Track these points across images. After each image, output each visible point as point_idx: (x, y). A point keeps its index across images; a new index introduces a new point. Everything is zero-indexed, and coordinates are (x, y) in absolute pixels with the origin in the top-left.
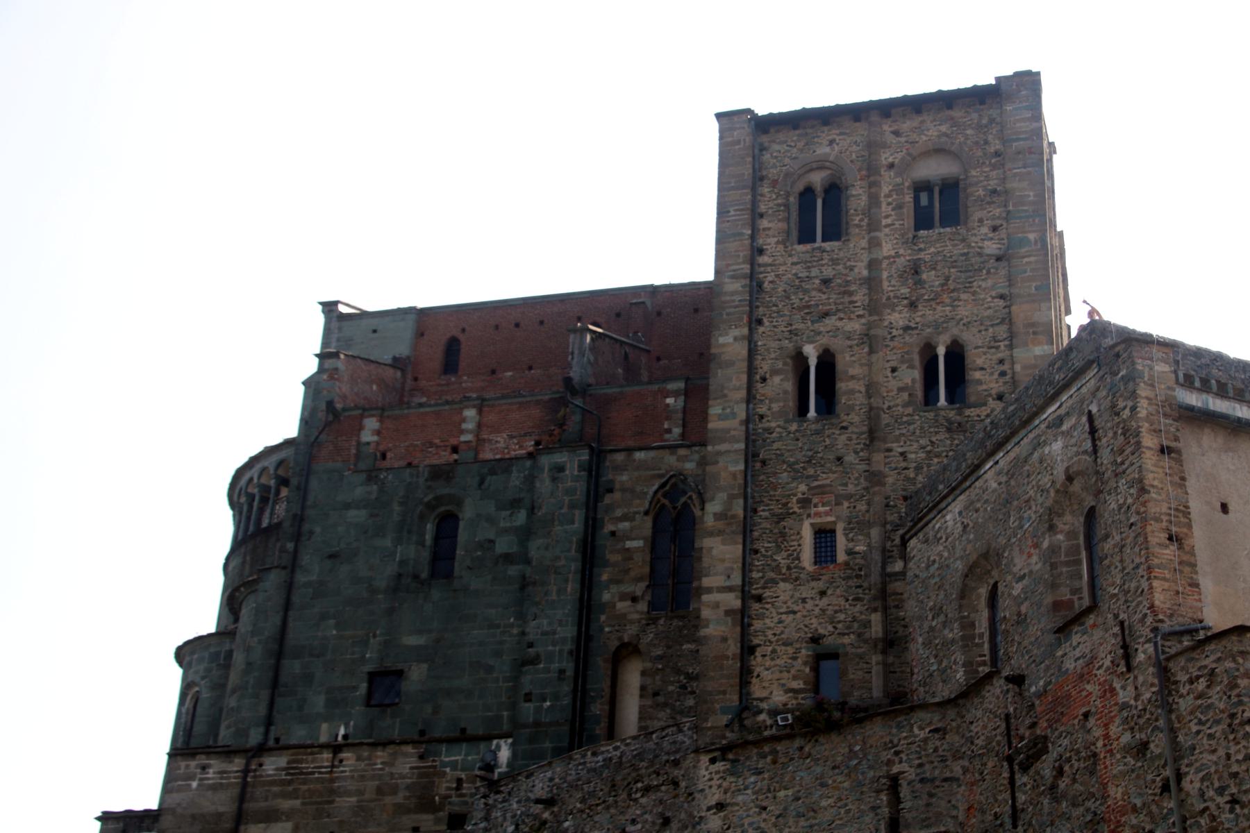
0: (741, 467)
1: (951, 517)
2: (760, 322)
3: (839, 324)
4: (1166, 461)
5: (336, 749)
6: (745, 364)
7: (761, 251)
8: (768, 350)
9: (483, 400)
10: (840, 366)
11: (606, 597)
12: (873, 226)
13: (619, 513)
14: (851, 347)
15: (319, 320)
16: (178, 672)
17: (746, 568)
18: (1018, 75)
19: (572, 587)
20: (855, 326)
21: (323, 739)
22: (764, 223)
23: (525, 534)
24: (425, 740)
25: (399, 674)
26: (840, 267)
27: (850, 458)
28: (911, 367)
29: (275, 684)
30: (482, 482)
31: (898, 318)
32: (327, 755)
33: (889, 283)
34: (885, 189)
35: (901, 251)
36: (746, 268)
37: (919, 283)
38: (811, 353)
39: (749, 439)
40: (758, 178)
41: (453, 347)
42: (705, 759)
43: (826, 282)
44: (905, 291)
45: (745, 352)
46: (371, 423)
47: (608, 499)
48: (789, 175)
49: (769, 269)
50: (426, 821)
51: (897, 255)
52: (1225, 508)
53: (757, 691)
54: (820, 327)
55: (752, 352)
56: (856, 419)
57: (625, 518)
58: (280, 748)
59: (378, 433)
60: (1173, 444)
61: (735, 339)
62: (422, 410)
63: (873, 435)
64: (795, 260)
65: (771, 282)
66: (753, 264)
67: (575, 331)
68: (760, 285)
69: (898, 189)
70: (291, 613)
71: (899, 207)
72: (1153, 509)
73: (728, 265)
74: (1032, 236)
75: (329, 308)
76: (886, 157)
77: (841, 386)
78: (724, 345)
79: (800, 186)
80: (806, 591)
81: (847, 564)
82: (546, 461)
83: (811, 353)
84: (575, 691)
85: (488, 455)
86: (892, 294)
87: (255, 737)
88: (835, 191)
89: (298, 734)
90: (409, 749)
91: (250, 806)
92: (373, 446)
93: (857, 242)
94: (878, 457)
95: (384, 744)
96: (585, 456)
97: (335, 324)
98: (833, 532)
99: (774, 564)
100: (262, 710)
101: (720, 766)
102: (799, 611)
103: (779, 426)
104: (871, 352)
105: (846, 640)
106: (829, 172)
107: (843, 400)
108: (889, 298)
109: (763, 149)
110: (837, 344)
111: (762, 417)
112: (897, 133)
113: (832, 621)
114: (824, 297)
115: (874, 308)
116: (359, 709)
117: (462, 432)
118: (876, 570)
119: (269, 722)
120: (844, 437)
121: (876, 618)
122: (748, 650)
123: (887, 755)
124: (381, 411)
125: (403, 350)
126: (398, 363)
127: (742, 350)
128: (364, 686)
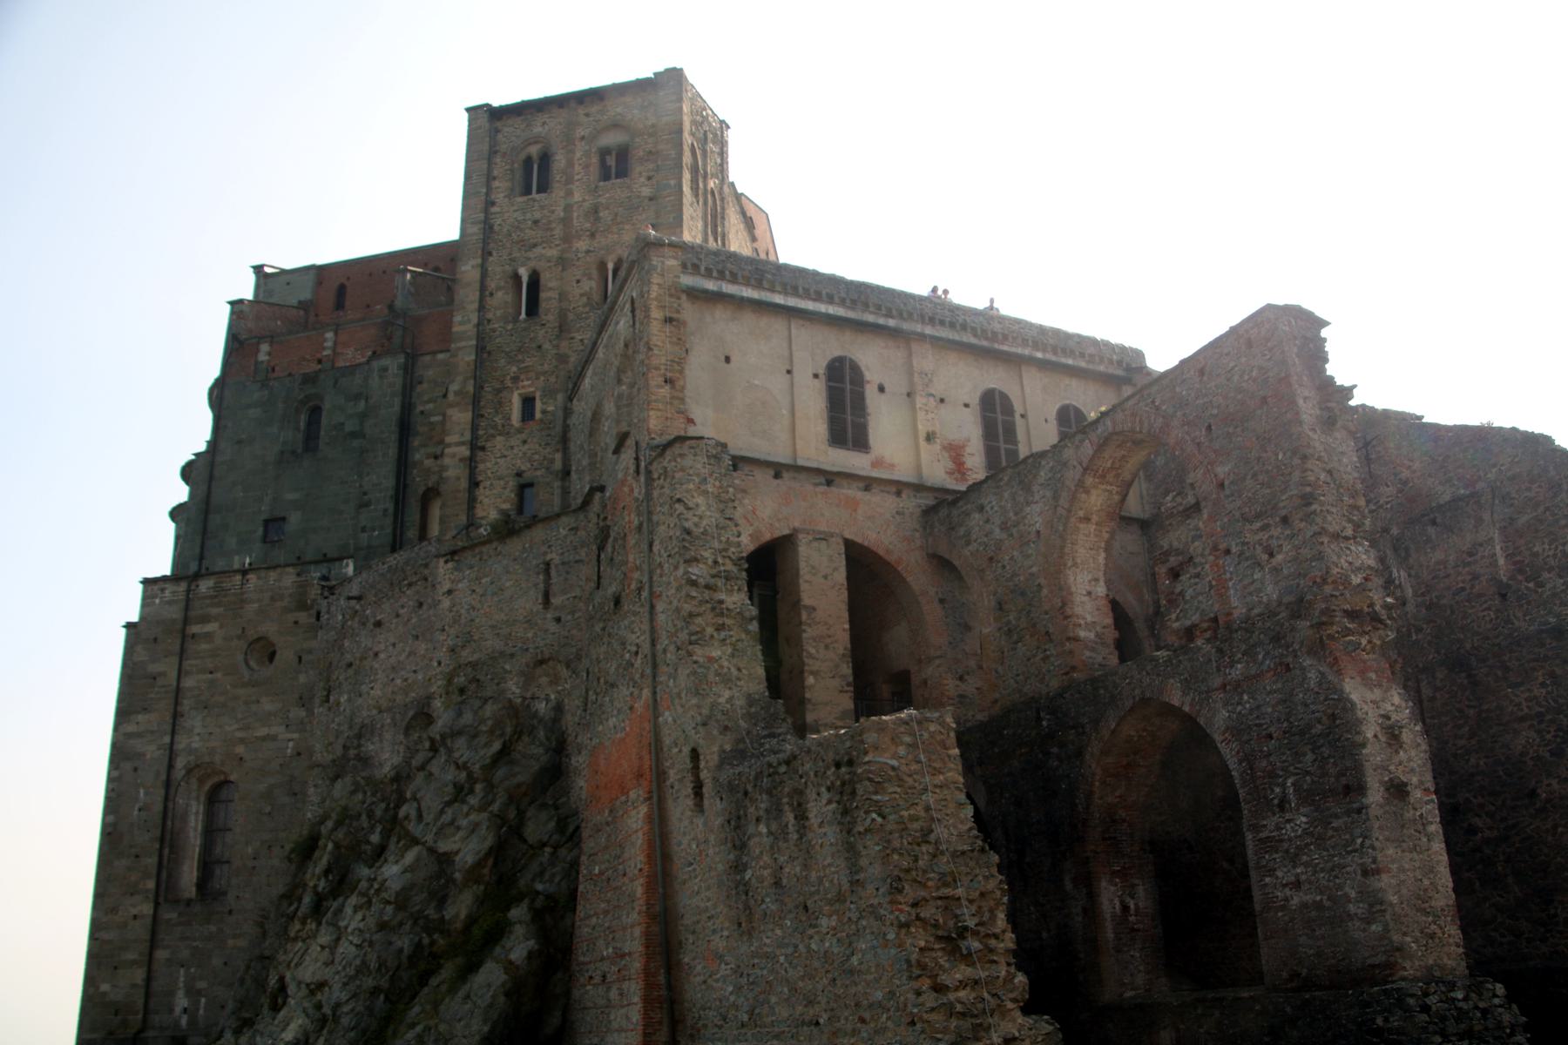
1: (587, 382)
2: (490, 254)
4: (668, 328)
5: (244, 572)
6: (477, 285)
7: (493, 204)
10: (542, 281)
11: (417, 457)
12: (570, 181)
13: (426, 398)
15: (251, 279)
16: (171, 527)
17: (474, 428)
18: (668, 71)
19: (393, 452)
20: (553, 253)
21: (236, 566)
22: (496, 184)
23: (363, 416)
24: (300, 563)
25: (283, 519)
27: (547, 346)
28: (590, 279)
29: (205, 531)
31: (582, 245)
32: (239, 577)
33: (578, 221)
34: (578, 155)
36: (482, 216)
37: (598, 219)
38: (524, 273)
39: (480, 337)
40: (493, 152)
41: (342, 290)
42: (442, 561)
43: (536, 222)
44: (588, 225)
46: (265, 347)
47: (419, 389)
48: (516, 148)
50: (303, 617)
52: (728, 360)
53: (480, 512)
54: (530, 255)
55: (484, 274)
56: (550, 317)
57: (429, 401)
58: (210, 574)
59: (269, 354)
60: (675, 316)
63: (563, 328)
66: (486, 211)
67: (399, 271)
68: (491, 227)
69: (587, 154)
71: (587, 167)
72: (655, 362)
74: (672, 182)
75: (258, 269)
76: (580, 132)
77: (543, 295)
79: (523, 156)
80: (514, 441)
82: (376, 364)
83: (524, 273)
84: (395, 522)
85: (340, 363)
87: (193, 567)
88: (545, 159)
89: (220, 564)
90: (290, 570)
91: (192, 613)
93: (558, 192)
94: (564, 344)
95: (275, 567)
96: (401, 359)
98: (533, 399)
100: (197, 550)
101: (450, 565)
102: (506, 459)
105: (539, 473)
107: (543, 305)
109: (497, 131)
110: (541, 266)
112: (587, 115)
113: (530, 460)
115: (567, 239)
118: (559, 422)
119: (201, 558)
121: (558, 456)
122: (474, 484)
123: (544, 548)
124: (271, 338)
125: (306, 295)
126: (303, 305)
127: (476, 274)
128: (261, 529)
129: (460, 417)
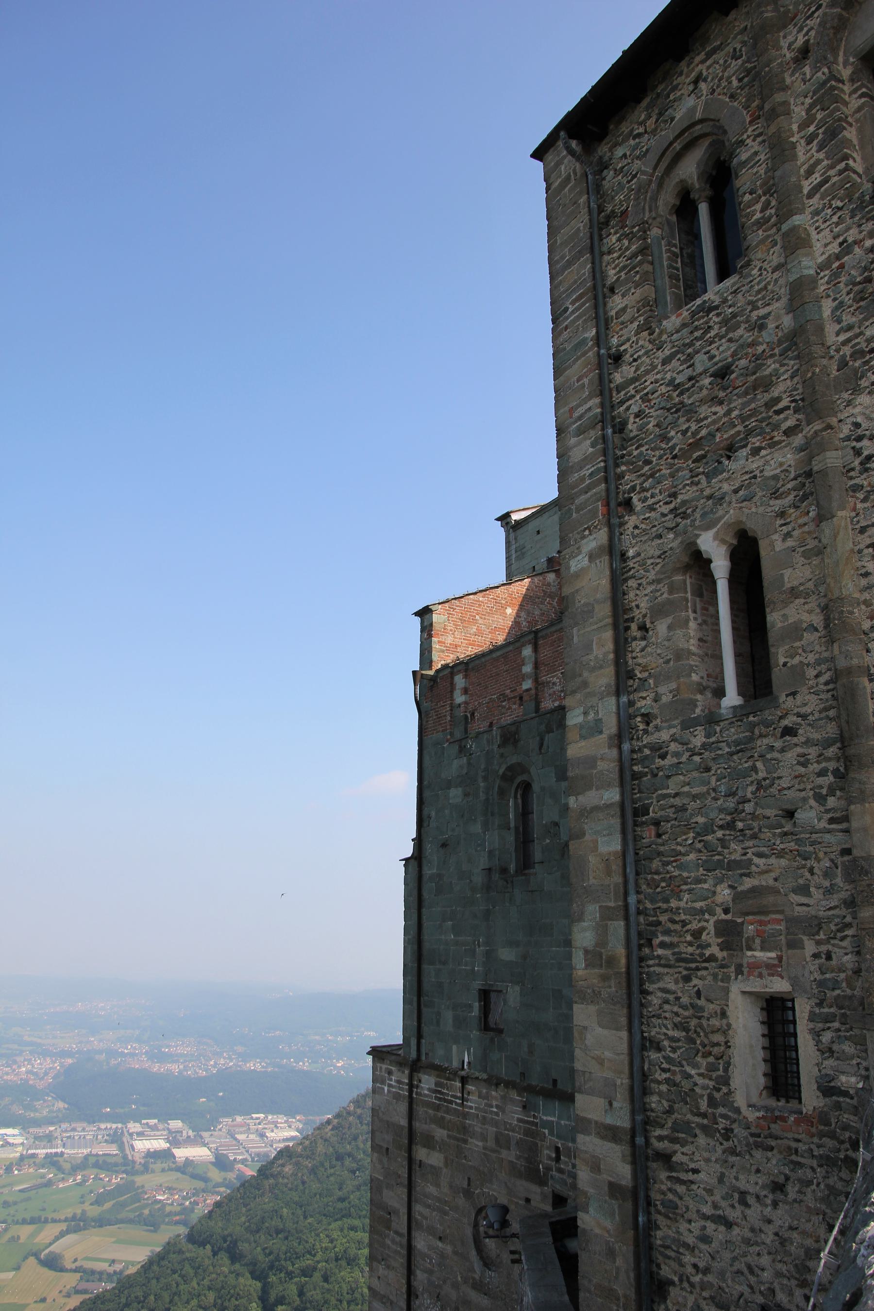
0: (616, 845)
2: (628, 504)
3: (754, 464)
7: (617, 358)
8: (643, 564)
9: (536, 632)
14: (782, 514)
15: (500, 533)
20: (784, 459)
22: (617, 302)
26: (740, 331)
30: (541, 745)
35: (852, 235)
43: (722, 374)
45: (605, 582)
46: (459, 680)
49: (631, 390)
51: (846, 248)
59: (465, 691)
61: (592, 557)
62: (494, 655)
64: (667, 352)
65: (637, 416)
66: (603, 388)
68: (620, 428)
70: (424, 910)
73: (572, 411)
75: (504, 519)
78: (577, 575)
79: (668, 198)
81: (823, 1118)
86: (847, 350)
92: (462, 708)
97: (512, 535)
99: (686, 1085)
103: (674, 739)
104: (820, 519)
106: (705, 143)
108: (843, 364)
111: (647, 718)
114: (720, 410)
116: (475, 1034)
117: (524, 677)
120: (791, 756)
129: (599, 1043)
